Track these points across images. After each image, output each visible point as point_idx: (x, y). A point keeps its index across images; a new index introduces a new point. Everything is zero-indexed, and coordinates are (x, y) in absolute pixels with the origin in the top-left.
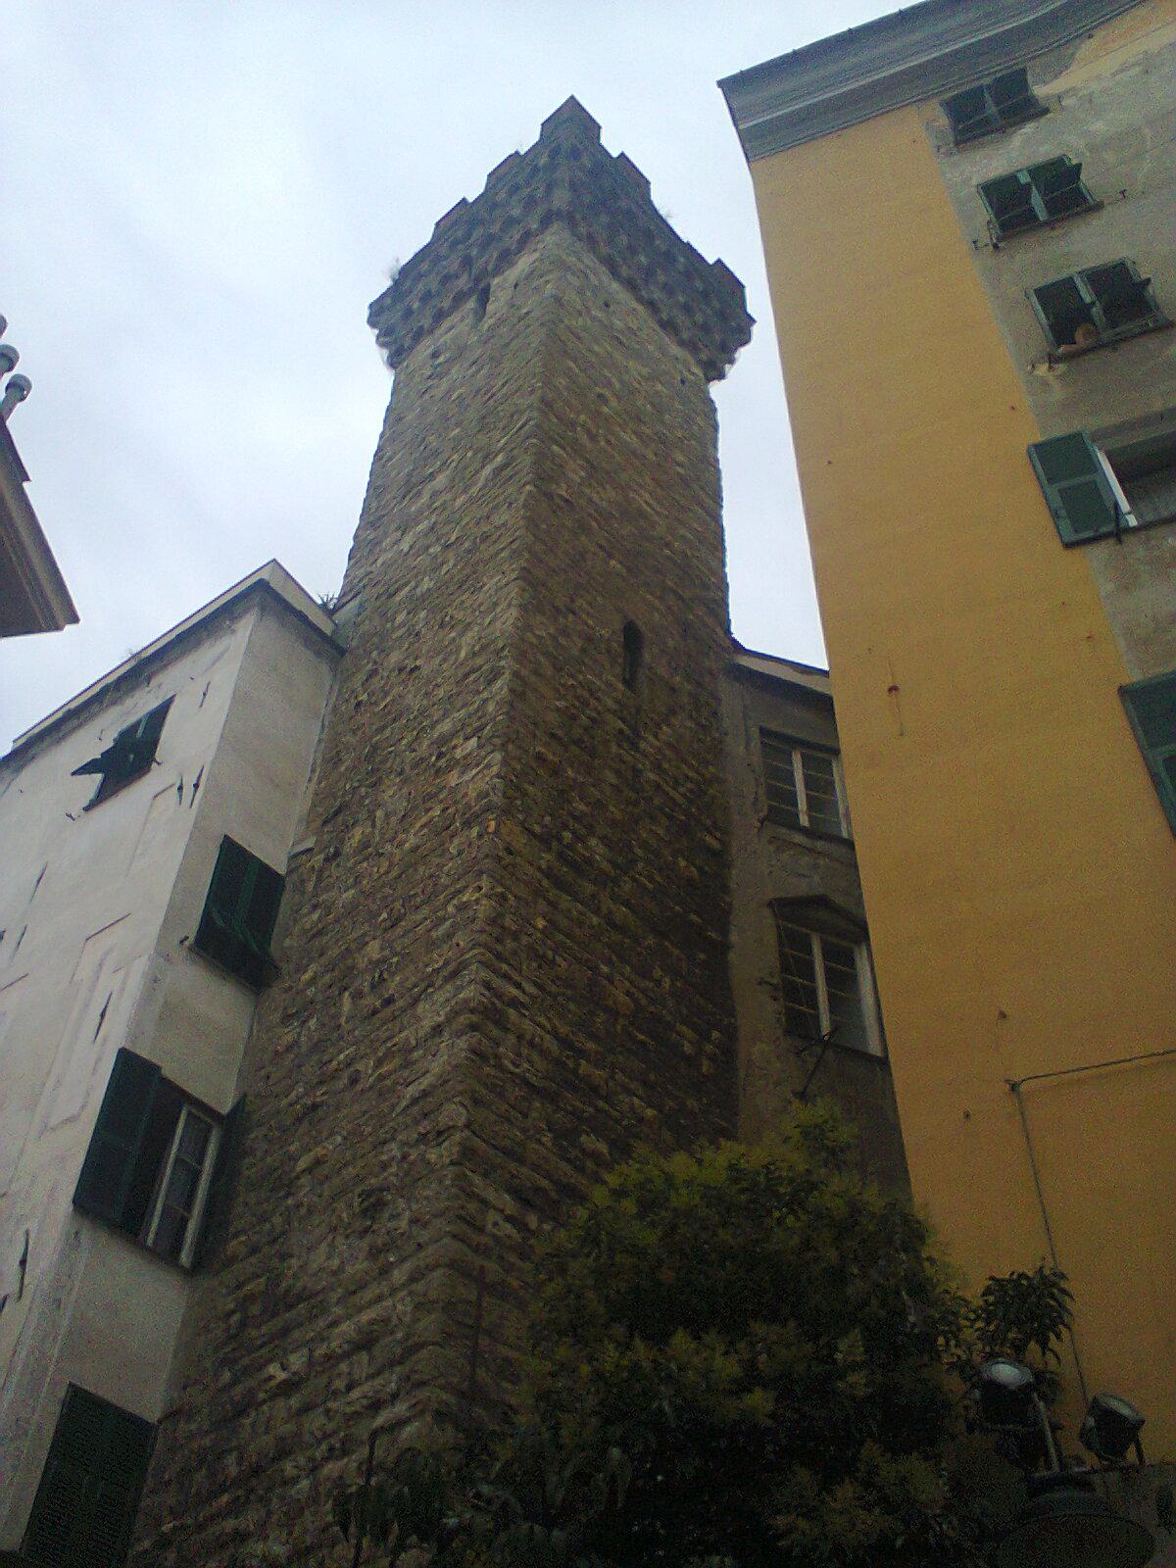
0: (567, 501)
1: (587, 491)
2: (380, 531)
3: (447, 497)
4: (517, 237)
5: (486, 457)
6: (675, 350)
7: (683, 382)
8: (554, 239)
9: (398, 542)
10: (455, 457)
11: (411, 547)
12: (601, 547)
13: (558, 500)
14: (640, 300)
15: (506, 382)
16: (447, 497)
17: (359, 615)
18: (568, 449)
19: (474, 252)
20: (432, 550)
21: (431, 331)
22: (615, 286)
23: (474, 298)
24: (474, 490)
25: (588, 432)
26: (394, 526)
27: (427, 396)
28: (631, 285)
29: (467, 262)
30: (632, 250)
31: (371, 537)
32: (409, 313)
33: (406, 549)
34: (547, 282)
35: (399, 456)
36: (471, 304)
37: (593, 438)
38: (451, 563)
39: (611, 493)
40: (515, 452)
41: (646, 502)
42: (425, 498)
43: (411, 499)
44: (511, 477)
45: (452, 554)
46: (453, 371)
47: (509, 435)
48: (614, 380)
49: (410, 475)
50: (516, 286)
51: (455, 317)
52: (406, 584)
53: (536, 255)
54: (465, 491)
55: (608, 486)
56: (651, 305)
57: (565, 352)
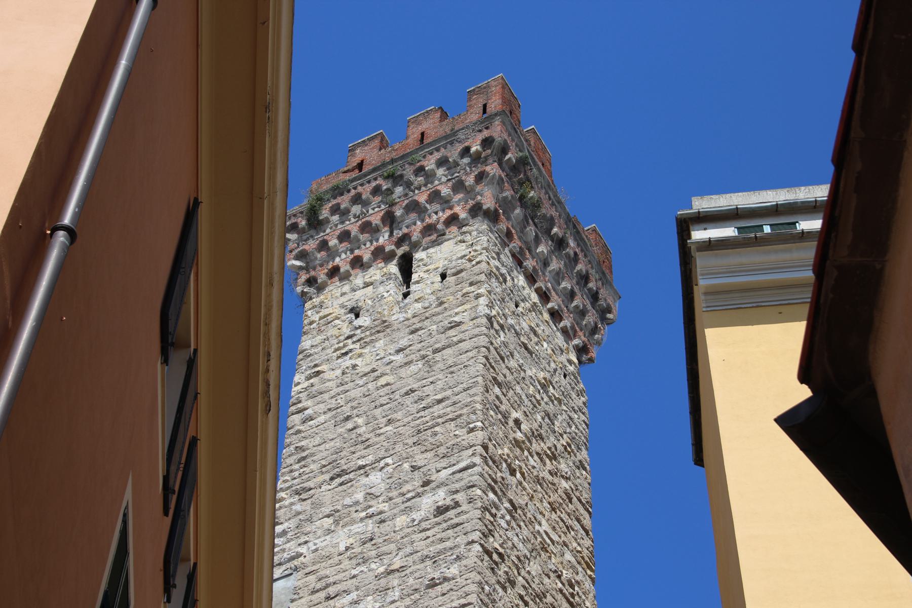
0: (501, 555)
1: (510, 534)
2: (307, 506)
3: (384, 507)
4: (444, 215)
5: (426, 484)
6: (560, 340)
7: (565, 376)
8: (480, 234)
9: (329, 531)
10: (389, 461)
11: (347, 549)
12: (521, 597)
13: (495, 556)
14: (538, 291)
15: (440, 401)
16: (384, 507)
17: (292, 601)
18: (500, 493)
19: (398, 213)
20: (373, 566)
21: (346, 277)
22: (521, 281)
23: (395, 262)
24: (417, 516)
25: (509, 466)
26: (327, 510)
27: (347, 362)
28: (531, 279)
29: (390, 219)
30: (537, 241)
31: (298, 507)
32: (324, 245)
33: (342, 548)
34: (478, 297)
35: (322, 418)
36: (393, 268)
37: (513, 472)
38: (397, 594)
39: (526, 532)
40: (460, 497)
41: (546, 533)
42: (360, 496)
43: (341, 484)
44: (458, 525)
45: (396, 582)
46: (378, 345)
47: (450, 470)
48: (524, 397)
49: (338, 451)
50: (443, 276)
51: (375, 273)
52: (347, 592)
53: (462, 249)
54: (408, 510)
55: (522, 524)
56: (544, 297)
57: (495, 379)
